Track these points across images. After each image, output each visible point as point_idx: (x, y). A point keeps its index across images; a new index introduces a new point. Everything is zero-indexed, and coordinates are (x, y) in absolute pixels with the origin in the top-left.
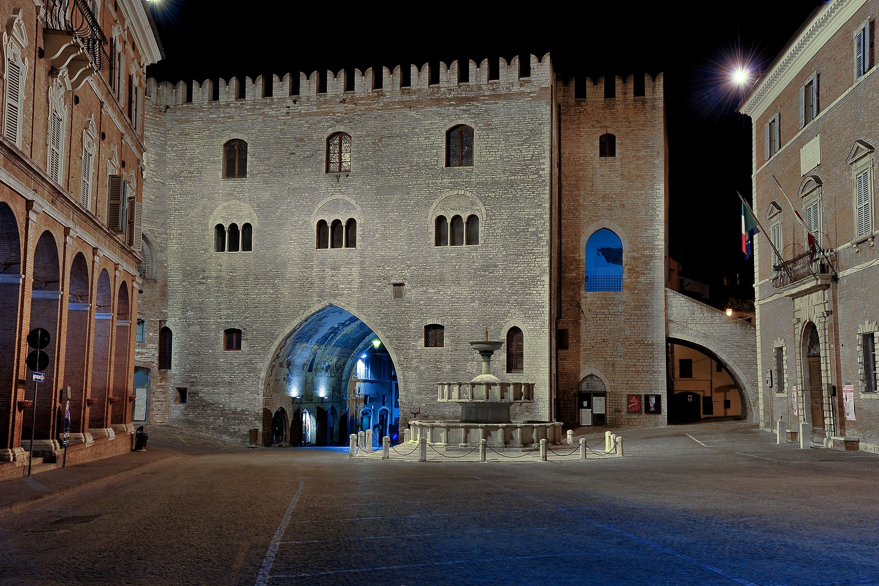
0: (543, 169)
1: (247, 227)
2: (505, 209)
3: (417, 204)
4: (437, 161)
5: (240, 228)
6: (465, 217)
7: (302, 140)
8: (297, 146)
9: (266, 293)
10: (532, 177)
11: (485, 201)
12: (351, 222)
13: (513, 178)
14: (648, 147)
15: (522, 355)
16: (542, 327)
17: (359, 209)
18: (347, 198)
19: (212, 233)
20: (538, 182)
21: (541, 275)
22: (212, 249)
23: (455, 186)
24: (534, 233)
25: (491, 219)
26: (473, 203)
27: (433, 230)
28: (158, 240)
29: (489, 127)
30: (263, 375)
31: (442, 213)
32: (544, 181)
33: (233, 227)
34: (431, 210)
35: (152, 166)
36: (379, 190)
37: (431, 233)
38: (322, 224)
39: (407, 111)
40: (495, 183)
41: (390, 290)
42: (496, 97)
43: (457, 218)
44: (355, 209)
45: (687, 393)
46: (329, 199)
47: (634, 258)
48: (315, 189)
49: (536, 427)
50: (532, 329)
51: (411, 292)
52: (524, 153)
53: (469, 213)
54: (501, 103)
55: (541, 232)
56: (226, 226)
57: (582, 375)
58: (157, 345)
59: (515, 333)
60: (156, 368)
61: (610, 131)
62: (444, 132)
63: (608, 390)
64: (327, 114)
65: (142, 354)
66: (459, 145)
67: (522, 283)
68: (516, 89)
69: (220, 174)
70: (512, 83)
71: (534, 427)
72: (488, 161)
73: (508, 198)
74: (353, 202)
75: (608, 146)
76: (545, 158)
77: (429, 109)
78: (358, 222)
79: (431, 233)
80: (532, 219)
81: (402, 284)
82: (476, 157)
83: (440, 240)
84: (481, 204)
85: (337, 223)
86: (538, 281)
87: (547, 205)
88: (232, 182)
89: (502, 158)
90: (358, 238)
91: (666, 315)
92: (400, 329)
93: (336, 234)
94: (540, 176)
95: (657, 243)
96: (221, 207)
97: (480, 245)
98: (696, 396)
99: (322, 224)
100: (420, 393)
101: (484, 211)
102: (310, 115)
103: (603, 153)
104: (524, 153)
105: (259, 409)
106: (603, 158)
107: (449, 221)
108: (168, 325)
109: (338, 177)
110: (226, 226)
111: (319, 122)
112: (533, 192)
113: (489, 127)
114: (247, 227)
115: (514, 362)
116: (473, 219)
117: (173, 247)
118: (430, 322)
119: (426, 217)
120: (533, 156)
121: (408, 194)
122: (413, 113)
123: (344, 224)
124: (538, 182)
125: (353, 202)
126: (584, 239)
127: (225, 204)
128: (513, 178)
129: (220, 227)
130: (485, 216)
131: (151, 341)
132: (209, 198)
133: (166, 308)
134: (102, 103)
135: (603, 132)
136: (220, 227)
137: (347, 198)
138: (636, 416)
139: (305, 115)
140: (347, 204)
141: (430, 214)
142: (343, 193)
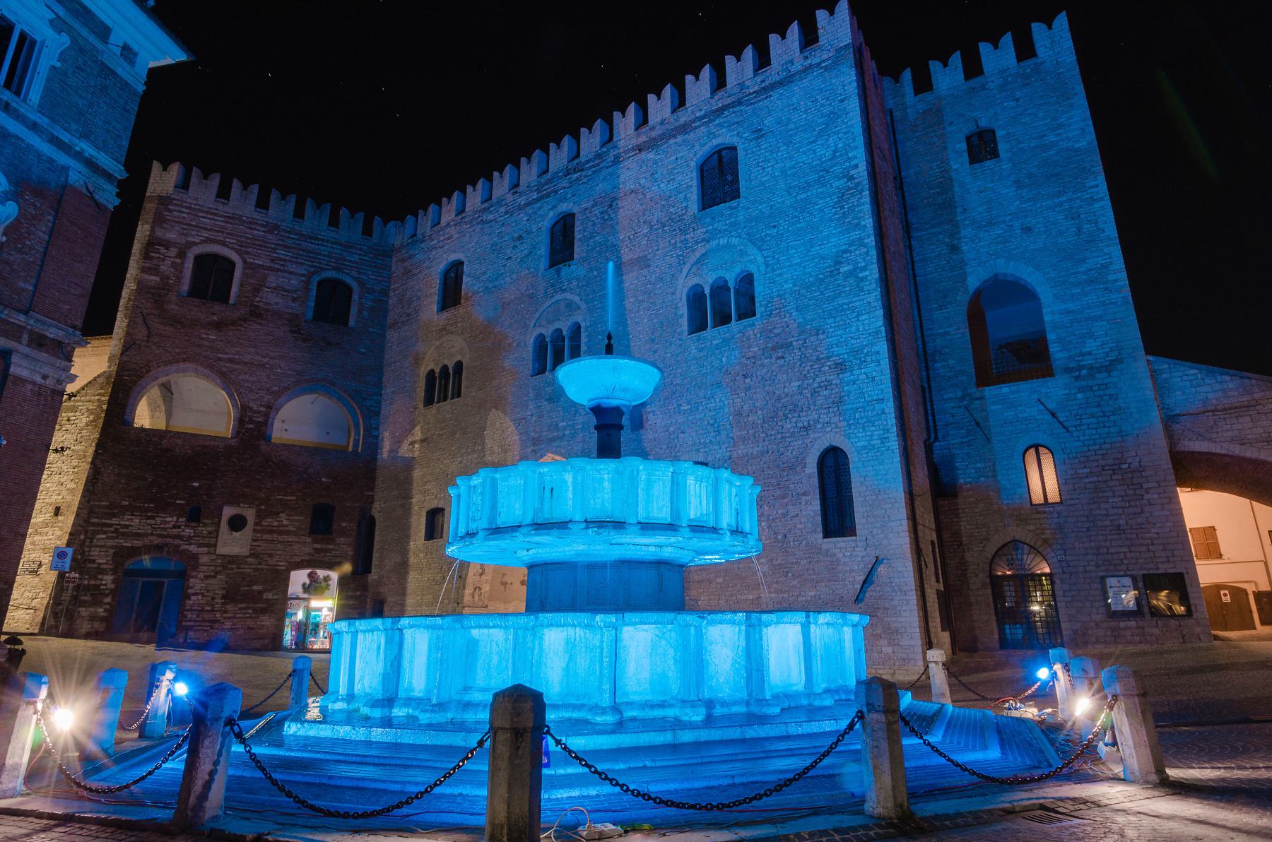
0: (856, 166)
1: (459, 366)
3: (660, 279)
4: (686, 207)
6: (731, 277)
7: (520, 237)
8: (515, 247)
10: (838, 183)
13: (804, 196)
14: (1061, 126)
16: (884, 440)
17: (583, 306)
18: (568, 296)
22: (421, 406)
25: (773, 270)
26: (742, 253)
27: (684, 310)
29: (759, 133)
32: (859, 184)
33: (445, 368)
34: (681, 281)
37: (682, 316)
39: (643, 155)
42: (766, 90)
45: (1219, 587)
46: (548, 303)
47: (1068, 312)
48: (531, 297)
50: (864, 448)
52: (820, 151)
53: (737, 270)
54: (775, 95)
55: (864, 269)
61: (983, 123)
62: (693, 164)
64: (548, 196)
66: (719, 178)
68: (797, 66)
69: (435, 308)
70: (792, 62)
72: (762, 184)
74: (576, 299)
75: (982, 146)
76: (857, 147)
77: (672, 141)
78: (583, 325)
79: (682, 316)
80: (845, 251)
82: (742, 183)
83: (698, 325)
84: (755, 251)
87: (869, 222)
88: (445, 315)
89: (783, 171)
91: (1162, 408)
94: (851, 178)
95: (1111, 277)
97: (758, 315)
98: (1238, 593)
101: (760, 259)
102: (528, 204)
103: (975, 158)
104: (820, 151)
106: (977, 165)
107: (707, 291)
110: (437, 370)
111: (539, 208)
112: (842, 207)
113: (759, 133)
114: (459, 366)
115: (837, 517)
120: (835, 152)
122: (651, 156)
124: (850, 189)
128: (804, 196)
130: (762, 268)
133: (372, 489)
135: (971, 128)
137: (568, 296)
138: (1132, 623)
139: (520, 208)
140: (570, 305)
141: (680, 287)
142: (564, 291)
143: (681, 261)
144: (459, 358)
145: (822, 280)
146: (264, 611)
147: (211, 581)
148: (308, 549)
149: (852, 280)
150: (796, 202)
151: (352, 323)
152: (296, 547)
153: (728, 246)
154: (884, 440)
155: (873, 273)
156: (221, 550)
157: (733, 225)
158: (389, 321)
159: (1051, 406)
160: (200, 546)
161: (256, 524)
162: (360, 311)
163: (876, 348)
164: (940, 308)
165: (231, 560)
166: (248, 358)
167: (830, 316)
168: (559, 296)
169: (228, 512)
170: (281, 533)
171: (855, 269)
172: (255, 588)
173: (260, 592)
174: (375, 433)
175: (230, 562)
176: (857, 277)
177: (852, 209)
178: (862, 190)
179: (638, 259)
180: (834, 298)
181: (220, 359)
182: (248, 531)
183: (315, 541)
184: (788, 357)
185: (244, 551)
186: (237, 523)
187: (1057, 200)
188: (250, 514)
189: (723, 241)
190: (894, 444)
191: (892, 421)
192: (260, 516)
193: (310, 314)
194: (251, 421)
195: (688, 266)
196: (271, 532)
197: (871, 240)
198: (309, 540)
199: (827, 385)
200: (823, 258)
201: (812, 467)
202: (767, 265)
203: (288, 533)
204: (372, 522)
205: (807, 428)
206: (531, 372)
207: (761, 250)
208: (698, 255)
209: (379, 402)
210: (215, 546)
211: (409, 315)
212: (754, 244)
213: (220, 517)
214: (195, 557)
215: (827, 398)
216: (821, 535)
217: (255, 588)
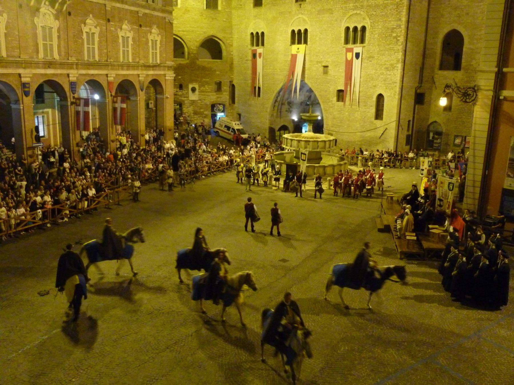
1: (263, 33)
2: (380, 22)
3: (336, 20)
5: (260, 34)
9: (270, 69)
11: (370, 17)
12: (306, 31)
13: (386, 2)
15: (383, 110)
17: (309, 23)
18: (304, 17)
19: (249, 37)
20: (400, 4)
21: (396, 64)
23: (356, 8)
24: (395, 37)
25: (373, 29)
26: (364, 19)
27: (343, 35)
28: (228, 42)
30: (269, 110)
31: (348, 25)
33: (257, 33)
34: (343, 23)
35: (224, 3)
36: (320, 12)
38: (293, 31)
40: (377, 6)
41: (321, 69)
43: (355, 28)
44: (307, 23)
46: (296, 18)
48: (290, 12)
49: (317, 167)
51: (331, 70)
53: (362, 25)
55: (399, 36)
56: (255, 33)
57: (431, 121)
58: (228, 93)
59: (380, 97)
60: (228, 104)
63: (444, 131)
65: (221, 97)
67: (387, 68)
69: (252, 5)
71: (315, 167)
73: (383, 15)
74: (307, 19)
78: (309, 30)
80: (395, 28)
81: (327, 67)
84: (368, 19)
85: (300, 31)
86: (395, 67)
87: (404, 19)
88: (258, 10)
90: (309, 40)
92: (326, 91)
93: (299, 37)
96: (252, 23)
99: (293, 31)
100: (332, 127)
101: (369, 23)
105: (267, 126)
107: (351, 30)
108: (234, 83)
109: (301, 5)
110: (255, 33)
115: (379, 115)
116: (364, 28)
117: (235, 44)
118: (339, 88)
119: (340, 27)
121: (332, 14)
123: (302, 32)
125: (307, 19)
126: (441, 37)
127: (254, 22)
128: (386, 2)
129: (252, 34)
130: (370, 26)
131: (225, 91)
132: (248, 19)
134: (105, 5)
136: (252, 34)
140: (304, 20)
141: (342, 26)
142: (302, 14)
143: (344, 14)
144: (263, 30)
145: (387, 37)
146: (205, 117)
147: (189, 108)
148: (215, 97)
149: (395, 40)
150: (383, 3)
151: (220, 8)
152: (211, 96)
153: (360, 14)
154: (395, 95)
155: (402, 39)
156: (190, 99)
157: (362, 6)
158: (233, 6)
159: (457, 81)
160: (185, 97)
161: (199, 89)
162: (222, 3)
163: (397, 65)
164: (433, 38)
165: (193, 102)
166: (188, 29)
167: (387, 51)
168: (300, 16)
169: (190, 86)
170: (206, 92)
171: (397, 36)
172: (202, 110)
173: (203, 112)
174: (232, 53)
175: (194, 102)
176: (397, 39)
177: (400, 12)
178: (404, 6)
179: (329, 9)
180: (389, 45)
181: (179, 31)
182: (197, 92)
183: (217, 94)
184: (373, 62)
185: (197, 99)
186: (193, 90)
187: (480, 4)
188: (197, 86)
189: (358, 12)
190: (397, 97)
191: (397, 89)
192: (200, 87)
193: (205, 8)
194: (192, 53)
195: (346, 18)
196: (204, 92)
197: (403, 27)
198: (215, 94)
199: (382, 74)
200: (388, 29)
201: (374, 99)
202: (371, 26)
203: (209, 92)
204: (233, 86)
205: (375, 86)
206: (290, 44)
207: (370, 19)
208: (349, 15)
209: (232, 41)
210: (188, 97)
211: (241, 5)
212: (368, 16)
213: (188, 88)
214: (184, 101)
215: (382, 78)
216: (373, 119)
217: (202, 110)
